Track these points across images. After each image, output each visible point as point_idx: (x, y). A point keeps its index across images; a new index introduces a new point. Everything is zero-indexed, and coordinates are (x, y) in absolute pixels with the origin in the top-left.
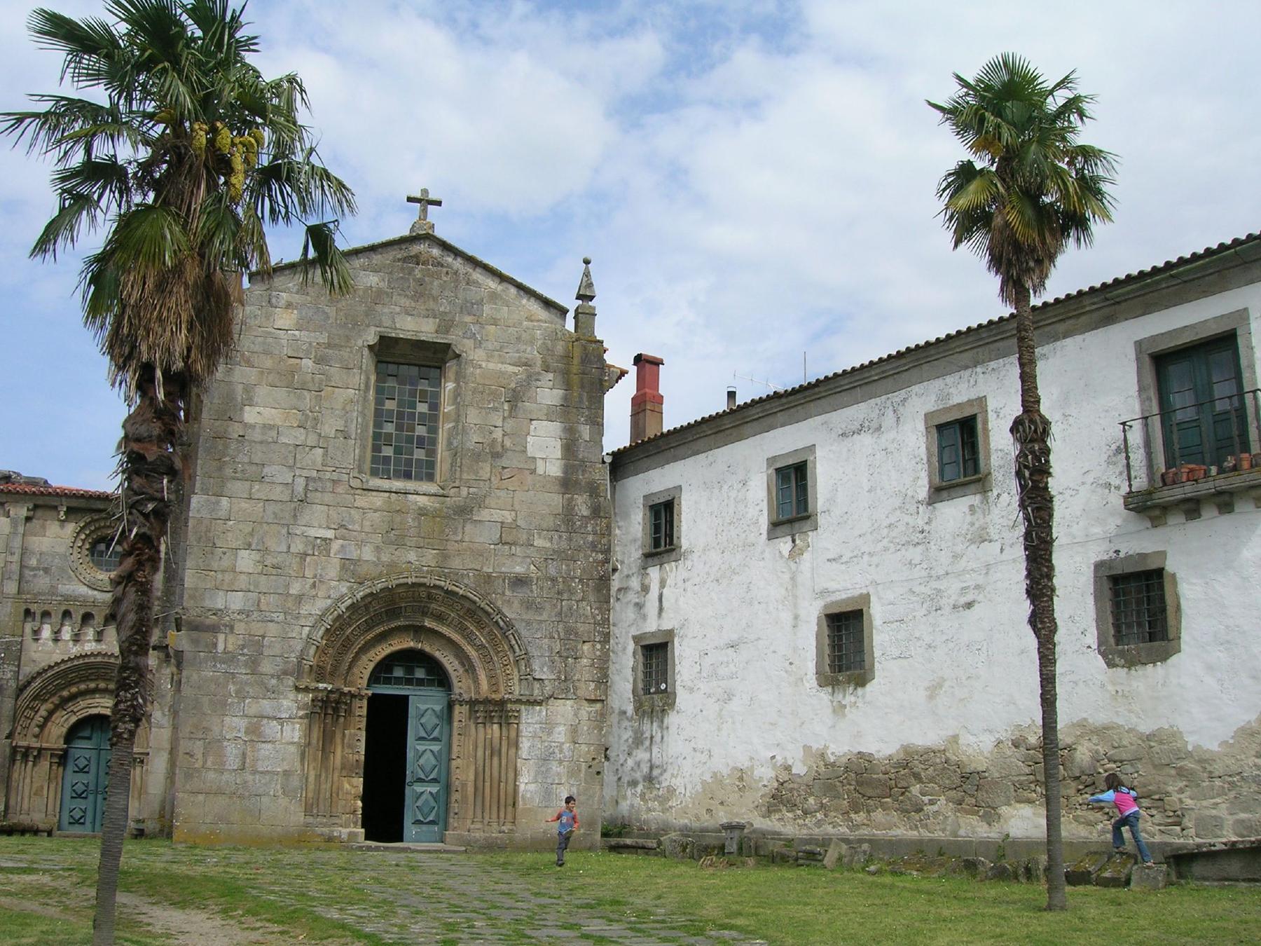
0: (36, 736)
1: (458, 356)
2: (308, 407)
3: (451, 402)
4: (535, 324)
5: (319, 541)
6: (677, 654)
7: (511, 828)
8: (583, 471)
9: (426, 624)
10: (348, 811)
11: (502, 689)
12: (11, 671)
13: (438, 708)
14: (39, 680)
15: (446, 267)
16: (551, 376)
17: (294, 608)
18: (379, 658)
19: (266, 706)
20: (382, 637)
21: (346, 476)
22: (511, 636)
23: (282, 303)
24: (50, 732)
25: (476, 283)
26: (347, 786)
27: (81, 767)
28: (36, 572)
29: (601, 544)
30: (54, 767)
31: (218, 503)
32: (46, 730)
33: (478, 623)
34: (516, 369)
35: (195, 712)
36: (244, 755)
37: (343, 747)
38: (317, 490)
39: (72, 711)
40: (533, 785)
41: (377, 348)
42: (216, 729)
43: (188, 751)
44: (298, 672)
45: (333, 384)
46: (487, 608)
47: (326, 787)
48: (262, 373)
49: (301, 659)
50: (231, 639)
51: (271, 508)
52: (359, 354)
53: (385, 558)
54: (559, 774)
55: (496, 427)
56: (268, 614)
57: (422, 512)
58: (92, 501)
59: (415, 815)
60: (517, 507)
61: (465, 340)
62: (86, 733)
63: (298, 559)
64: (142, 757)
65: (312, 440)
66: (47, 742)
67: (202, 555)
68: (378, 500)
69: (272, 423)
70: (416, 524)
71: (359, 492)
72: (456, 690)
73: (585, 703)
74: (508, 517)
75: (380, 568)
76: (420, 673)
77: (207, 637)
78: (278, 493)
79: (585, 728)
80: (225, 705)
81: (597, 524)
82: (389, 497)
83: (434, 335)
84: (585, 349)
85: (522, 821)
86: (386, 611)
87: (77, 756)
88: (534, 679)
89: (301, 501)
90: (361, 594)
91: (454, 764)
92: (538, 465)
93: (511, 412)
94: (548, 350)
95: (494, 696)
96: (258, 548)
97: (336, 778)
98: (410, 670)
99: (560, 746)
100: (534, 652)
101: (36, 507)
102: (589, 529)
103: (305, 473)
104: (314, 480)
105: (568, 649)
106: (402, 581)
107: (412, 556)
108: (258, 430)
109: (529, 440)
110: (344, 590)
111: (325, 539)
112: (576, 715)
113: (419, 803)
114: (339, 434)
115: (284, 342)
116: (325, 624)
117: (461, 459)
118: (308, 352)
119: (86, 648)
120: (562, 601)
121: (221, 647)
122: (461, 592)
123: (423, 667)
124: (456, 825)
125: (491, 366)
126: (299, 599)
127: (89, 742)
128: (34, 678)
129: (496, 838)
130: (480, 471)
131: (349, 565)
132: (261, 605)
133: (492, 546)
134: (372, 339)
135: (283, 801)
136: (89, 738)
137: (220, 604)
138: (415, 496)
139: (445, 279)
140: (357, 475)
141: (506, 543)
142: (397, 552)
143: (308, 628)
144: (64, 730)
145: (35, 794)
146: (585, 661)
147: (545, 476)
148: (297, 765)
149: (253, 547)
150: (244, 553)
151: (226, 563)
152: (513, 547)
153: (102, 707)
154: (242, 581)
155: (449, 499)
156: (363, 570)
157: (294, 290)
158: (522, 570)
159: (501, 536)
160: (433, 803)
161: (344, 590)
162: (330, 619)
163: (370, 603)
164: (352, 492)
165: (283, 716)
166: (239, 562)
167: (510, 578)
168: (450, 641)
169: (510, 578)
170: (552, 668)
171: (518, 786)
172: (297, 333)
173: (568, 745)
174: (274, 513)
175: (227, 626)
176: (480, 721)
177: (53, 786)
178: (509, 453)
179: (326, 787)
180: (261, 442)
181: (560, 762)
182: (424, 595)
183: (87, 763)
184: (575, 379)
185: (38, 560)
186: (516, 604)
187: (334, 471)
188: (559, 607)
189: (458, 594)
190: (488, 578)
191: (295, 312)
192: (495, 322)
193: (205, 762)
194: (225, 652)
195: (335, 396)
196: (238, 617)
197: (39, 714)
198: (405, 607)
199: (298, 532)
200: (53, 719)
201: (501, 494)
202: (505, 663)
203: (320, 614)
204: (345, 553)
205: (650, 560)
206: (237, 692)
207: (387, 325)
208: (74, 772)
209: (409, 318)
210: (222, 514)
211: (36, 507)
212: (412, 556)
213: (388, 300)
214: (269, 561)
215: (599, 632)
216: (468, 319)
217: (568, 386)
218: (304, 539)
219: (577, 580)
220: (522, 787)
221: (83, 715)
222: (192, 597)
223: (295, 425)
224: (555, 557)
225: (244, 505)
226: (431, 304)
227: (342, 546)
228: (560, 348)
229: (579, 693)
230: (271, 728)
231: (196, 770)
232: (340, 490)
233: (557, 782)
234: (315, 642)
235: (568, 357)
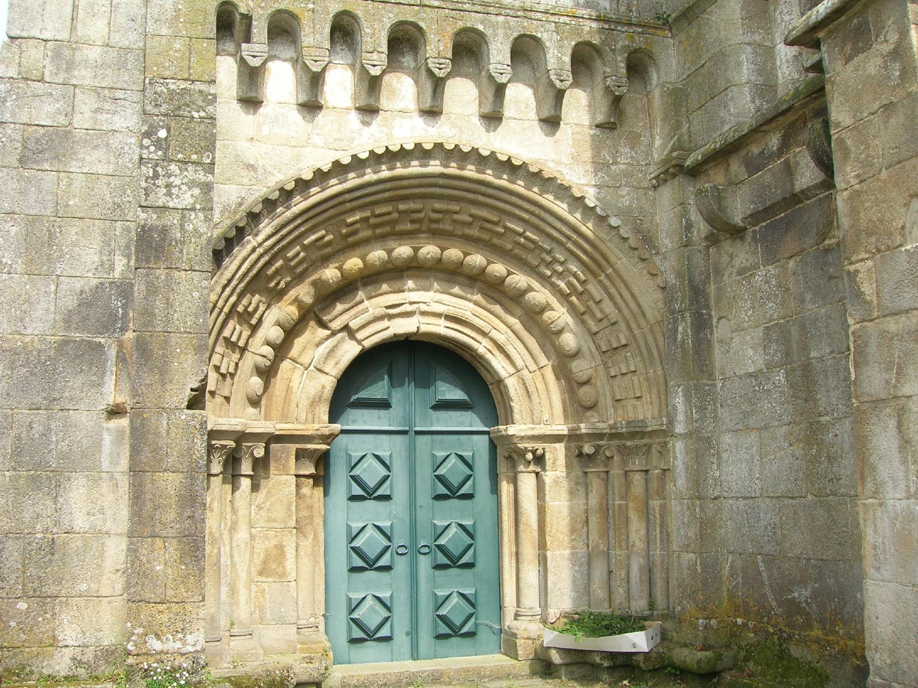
0: (255, 402)
12: (192, 184)
14: (266, 227)
24: (289, 389)
27: (372, 483)
30: (306, 490)
32: (278, 384)
39: (346, 328)
62: (377, 390)
64: (539, 446)
66: (284, 418)
87: (357, 455)
127: (383, 413)
128: (254, 217)
136: (384, 405)
144: (328, 383)
145: (261, 573)
153: (424, 313)
177: (307, 543)
183: (384, 472)
197: (261, 334)
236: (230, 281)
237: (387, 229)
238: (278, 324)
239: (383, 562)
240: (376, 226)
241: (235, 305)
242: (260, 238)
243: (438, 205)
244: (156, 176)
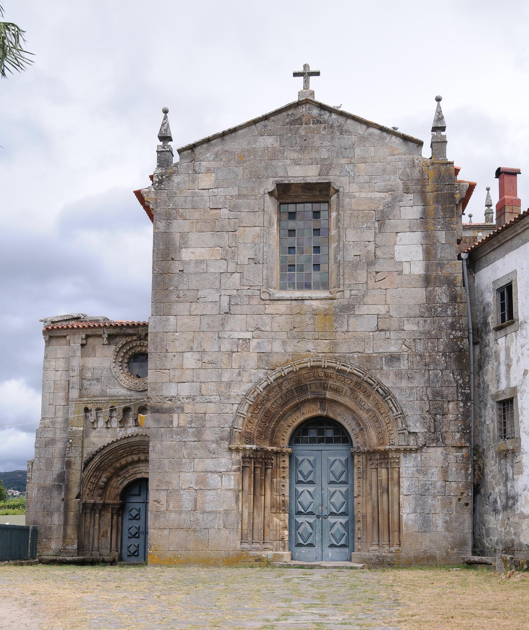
1: (337, 191)
2: (228, 244)
3: (335, 227)
4: (397, 157)
5: (241, 341)
6: (519, 406)
7: (397, 548)
8: (441, 268)
9: (327, 396)
10: (278, 538)
11: (387, 441)
13: (343, 459)
15: (323, 123)
16: (411, 196)
17: (226, 391)
18: (295, 424)
19: (210, 464)
20: (297, 408)
21: (258, 292)
22: (389, 401)
23: (203, 170)
25: (348, 131)
26: (276, 520)
28: (91, 382)
29: (459, 324)
31: (168, 320)
33: (365, 392)
34: (383, 195)
35: (160, 471)
36: (196, 500)
37: (271, 491)
38: (237, 304)
40: (414, 515)
41: (276, 193)
42: (175, 482)
43: (156, 499)
44: (230, 438)
45: (244, 225)
46: (369, 380)
47: (258, 521)
48: (193, 223)
49: (232, 428)
50: (182, 416)
51: (205, 320)
52: (262, 200)
53: (290, 349)
54: (433, 506)
55: (369, 242)
56: (207, 397)
57: (315, 313)
58: (124, 329)
59: (330, 540)
60: (389, 301)
61: (342, 178)
63: (227, 356)
65: (232, 267)
67: (159, 359)
68: (282, 307)
69: (202, 258)
70: (312, 322)
71: (267, 302)
72: (355, 445)
73: (453, 450)
74: (382, 310)
75: (287, 357)
76: (329, 433)
77: (165, 416)
78: (210, 309)
79: (454, 469)
80: (181, 465)
81: (455, 309)
82: (291, 304)
83: (318, 178)
84: (439, 171)
85: (406, 542)
86: (295, 388)
88: (409, 432)
89: (227, 313)
90: (274, 377)
91: (356, 500)
92: (404, 267)
93: (380, 229)
94: (408, 176)
95: (379, 448)
96: (198, 350)
97: (266, 514)
98: (321, 432)
99: (435, 484)
100: (408, 411)
101: (88, 336)
102: (449, 312)
103: (229, 292)
104: (235, 297)
105: (436, 408)
106: (302, 365)
107: (310, 346)
108: (192, 264)
109: (396, 249)
110: (261, 375)
111: (244, 340)
112: (445, 459)
113: (333, 531)
114: (251, 261)
115: (207, 198)
116: (249, 402)
117: (344, 270)
118: (224, 203)
119: (128, 432)
120: (429, 370)
121: (175, 424)
122: (348, 370)
123: (331, 428)
124: (359, 547)
125: (363, 195)
126: (229, 384)
129: (386, 557)
130: (359, 277)
131: (262, 356)
132: (202, 391)
133: (371, 333)
134: (271, 187)
135: (225, 533)
136: (139, 495)
137: (173, 393)
138: (310, 301)
139: (323, 133)
140: (266, 290)
141: (382, 330)
142: (299, 344)
143: (237, 405)
146: (451, 416)
147: (410, 275)
148: (234, 505)
149: (194, 350)
150: (188, 355)
151: (175, 363)
152: (388, 333)
154: (188, 375)
155: (336, 300)
156: (274, 360)
157: (211, 159)
158: (396, 349)
159: (377, 325)
160: (343, 531)
161: (261, 375)
162: (251, 397)
163: (282, 383)
164: (263, 302)
165: (222, 470)
166: (185, 361)
167: (386, 357)
168: (347, 407)
169: (386, 357)
170: (423, 424)
171: (402, 516)
172: (216, 190)
173: (440, 483)
174: (208, 324)
175: (179, 408)
176: (373, 467)
178: (381, 261)
179: (258, 521)
180: (195, 274)
181: (435, 497)
182: (322, 374)
184: (430, 196)
185: (92, 374)
186: (392, 375)
187: (250, 289)
188: (427, 376)
189: (346, 371)
190: (369, 359)
191: (213, 175)
192: (364, 161)
193: (168, 506)
194: (178, 427)
195: (246, 233)
196: (187, 401)
197: (101, 480)
198: (310, 385)
199: (226, 336)
200: (112, 483)
201: (376, 293)
202: (387, 422)
203: (245, 394)
204: (261, 348)
205: (498, 332)
206: (189, 454)
207: (282, 175)
208: (130, 519)
209: (298, 167)
210: (171, 328)
211: (88, 336)
212: (310, 346)
213: (281, 155)
214: (206, 359)
215: (462, 394)
216: (343, 161)
217: (425, 203)
218: (230, 341)
219: (440, 354)
220: (404, 517)
221: (131, 480)
222: (153, 389)
223: (219, 258)
224: (422, 337)
225: (186, 320)
226: (314, 154)
227: (258, 343)
228: (416, 174)
229: (448, 442)
230: (214, 480)
231: (164, 512)
232: (255, 301)
233: (433, 512)
234: (242, 415)
235: (422, 181)
236: (90, 469)
237: (131, 453)
238: (105, 477)
239: (137, 535)
240: (127, 453)
241: (92, 474)
242: (97, 459)
243: (142, 447)
244: (69, 450)
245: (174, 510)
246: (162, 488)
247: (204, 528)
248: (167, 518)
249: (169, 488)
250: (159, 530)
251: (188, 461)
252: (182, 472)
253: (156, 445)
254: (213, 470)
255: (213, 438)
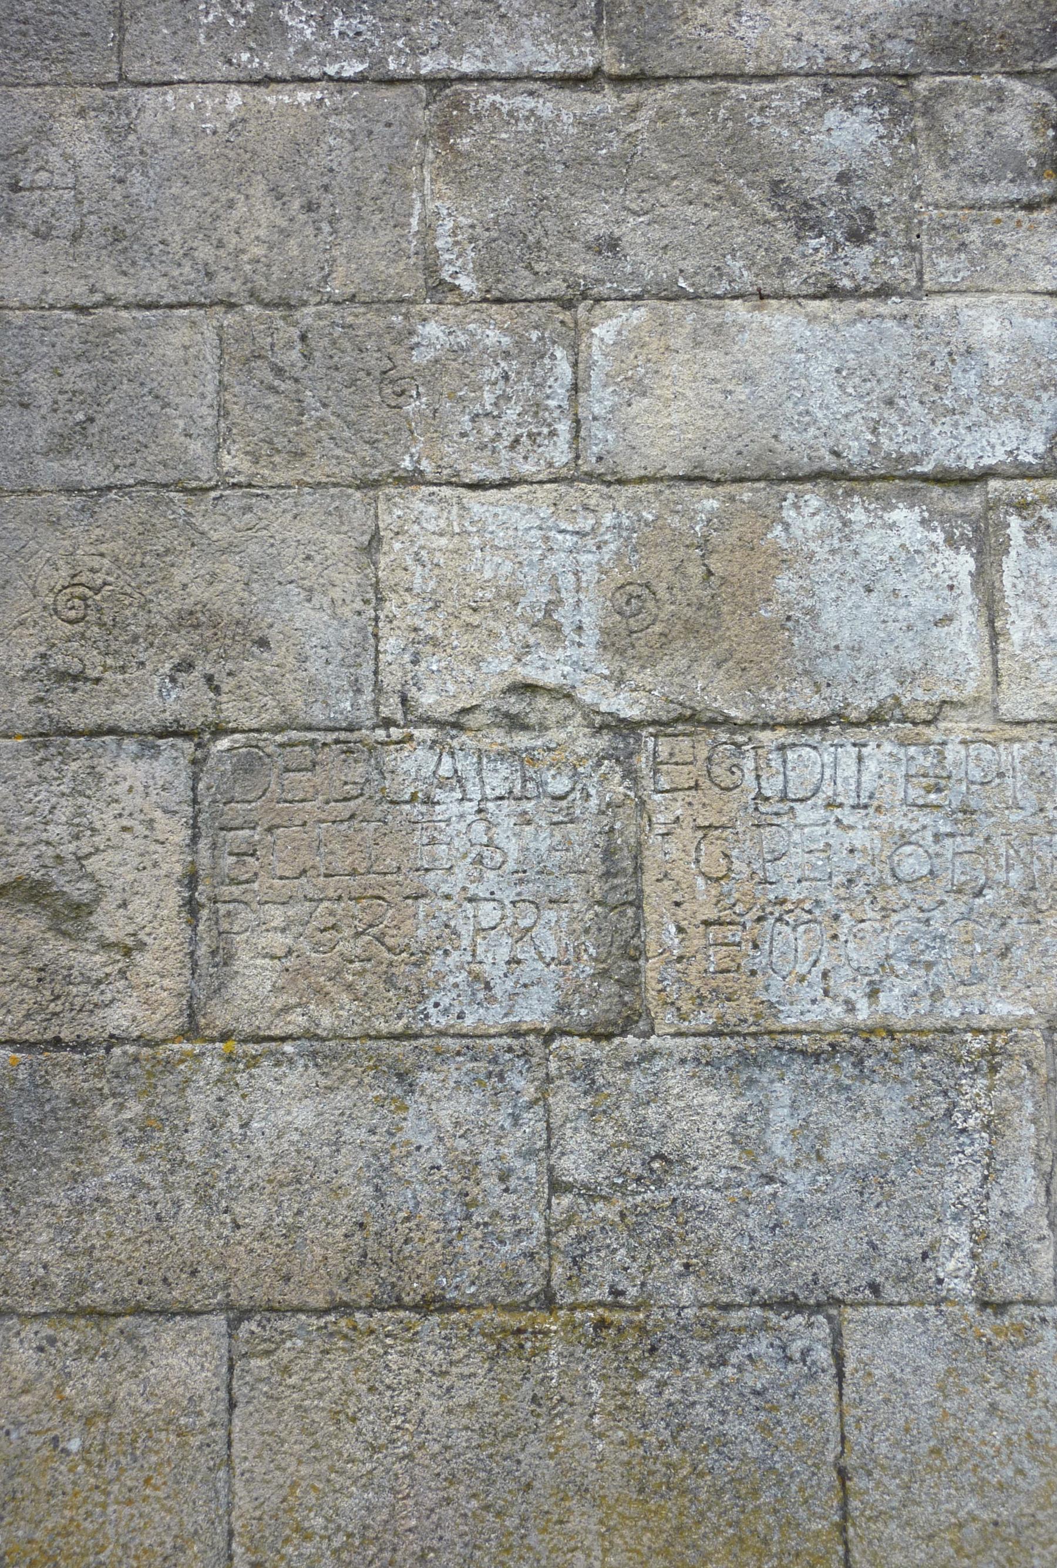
245: (297, 1021)
246: (121, 713)
247: (767, 1284)
248: (193, 1143)
249: (231, 711)
250: (69, 1336)
251: (493, 336)
252: (413, 479)
253: (42, 133)
254: (854, 450)
255: (835, 40)
